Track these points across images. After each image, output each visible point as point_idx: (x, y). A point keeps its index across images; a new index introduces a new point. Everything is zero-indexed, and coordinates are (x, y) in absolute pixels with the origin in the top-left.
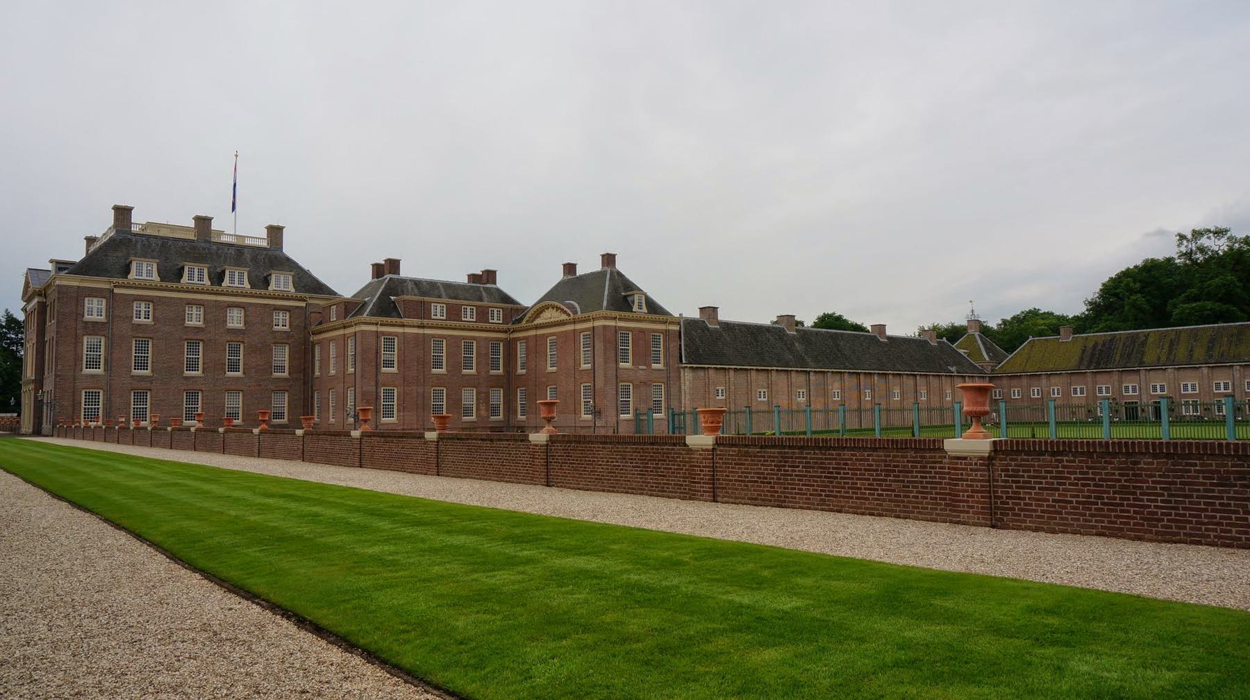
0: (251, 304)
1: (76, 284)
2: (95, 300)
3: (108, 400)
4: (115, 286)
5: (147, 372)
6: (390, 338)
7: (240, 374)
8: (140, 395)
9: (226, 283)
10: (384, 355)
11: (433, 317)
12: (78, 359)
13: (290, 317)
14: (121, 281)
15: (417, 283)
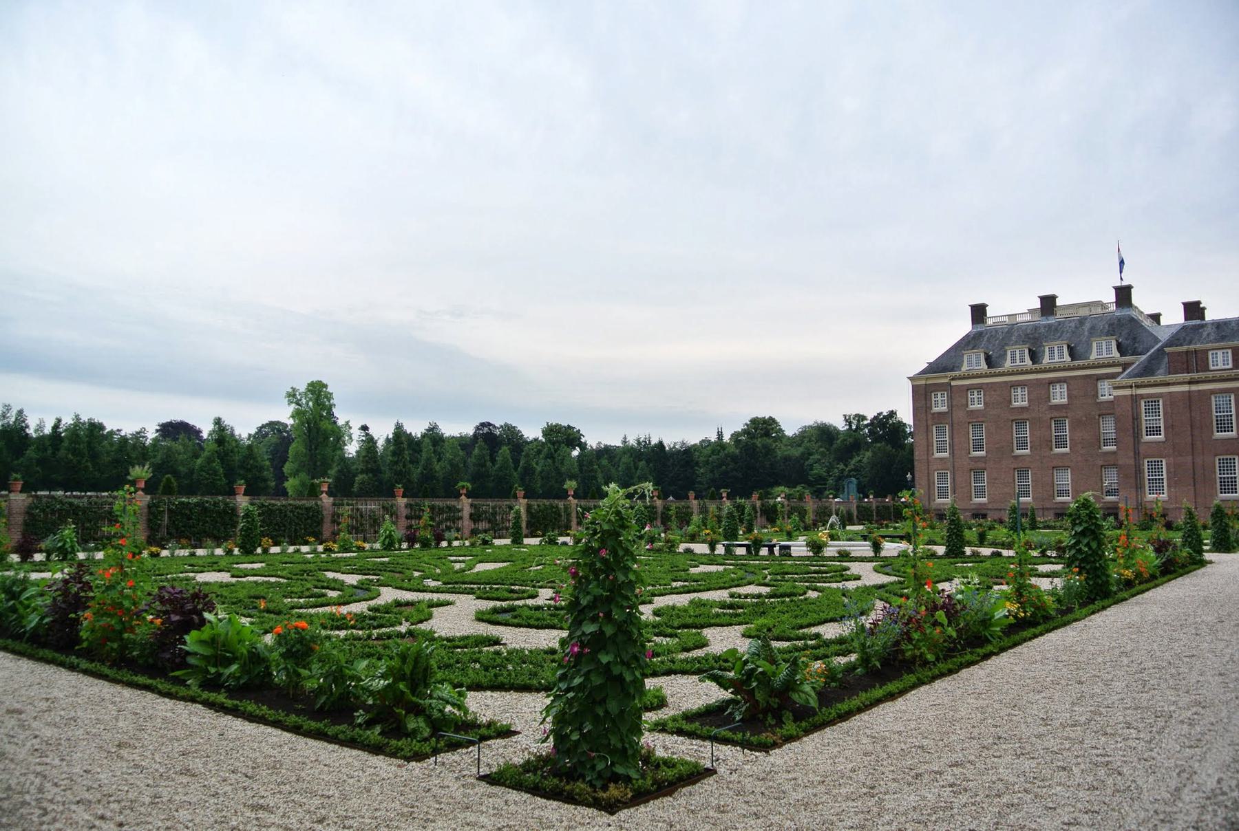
0: (1070, 377)
1: (923, 382)
2: (939, 394)
3: (954, 479)
4: (952, 379)
5: (983, 453)
6: (1152, 400)
7: (1067, 450)
8: (978, 473)
9: (1046, 360)
10: (1145, 420)
11: (1212, 368)
12: (929, 445)
13: (1068, 390)
14: (953, 374)
15: (1220, 325)
